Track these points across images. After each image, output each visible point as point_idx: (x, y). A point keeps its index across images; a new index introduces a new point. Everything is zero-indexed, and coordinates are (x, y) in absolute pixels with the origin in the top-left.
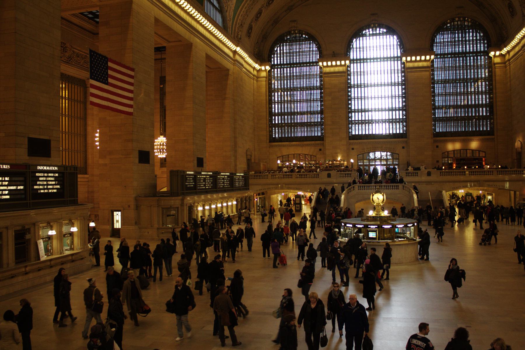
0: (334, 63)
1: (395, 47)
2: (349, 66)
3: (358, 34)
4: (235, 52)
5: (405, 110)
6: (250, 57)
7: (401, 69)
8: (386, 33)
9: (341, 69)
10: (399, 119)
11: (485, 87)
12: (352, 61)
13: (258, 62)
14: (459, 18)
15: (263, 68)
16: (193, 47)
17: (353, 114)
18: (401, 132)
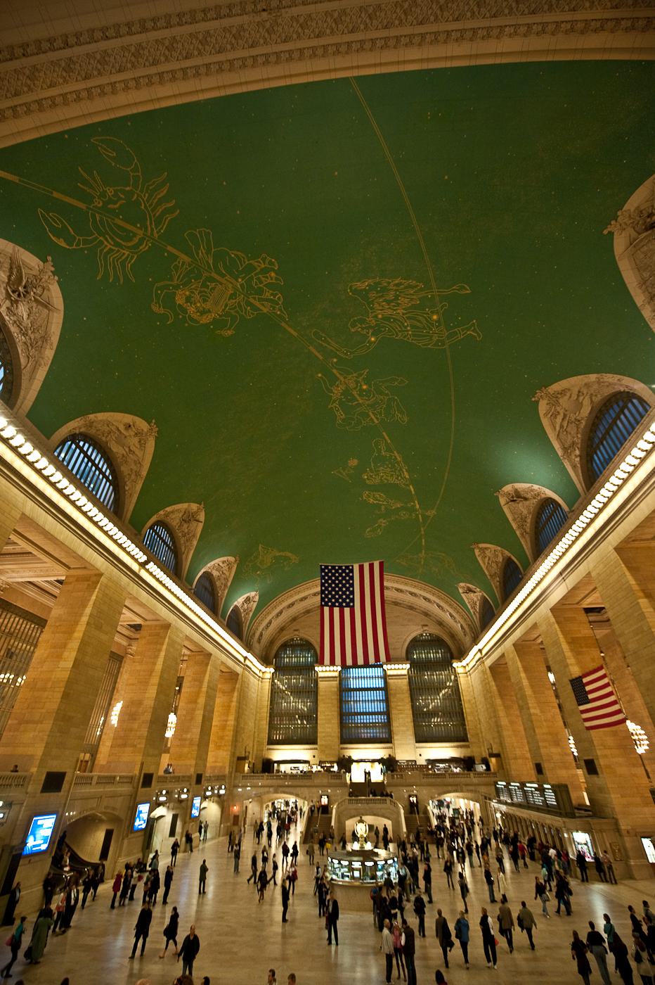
4: (246, 658)
14: (426, 634)
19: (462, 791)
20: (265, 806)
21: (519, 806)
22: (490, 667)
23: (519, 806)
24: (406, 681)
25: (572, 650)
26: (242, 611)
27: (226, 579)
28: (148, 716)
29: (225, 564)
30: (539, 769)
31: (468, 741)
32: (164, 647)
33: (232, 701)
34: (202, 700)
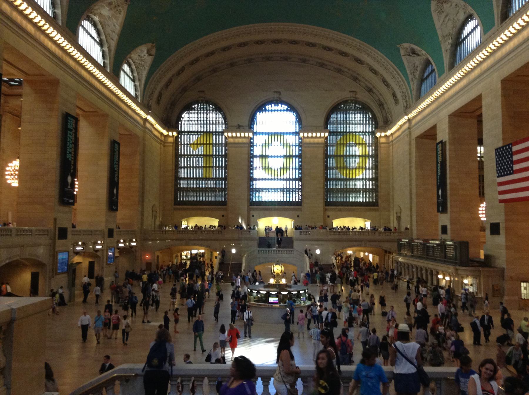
0: (238, 135)
1: (294, 123)
2: (253, 139)
3: (261, 108)
4: (146, 120)
5: (301, 181)
6: (159, 124)
7: (299, 144)
8: (287, 110)
9: (245, 141)
10: (296, 188)
11: (372, 163)
12: (255, 133)
13: (167, 128)
15: (170, 134)
17: (254, 182)
18: (297, 200)
20: (174, 255)
29: (112, 6)
31: (377, 206)
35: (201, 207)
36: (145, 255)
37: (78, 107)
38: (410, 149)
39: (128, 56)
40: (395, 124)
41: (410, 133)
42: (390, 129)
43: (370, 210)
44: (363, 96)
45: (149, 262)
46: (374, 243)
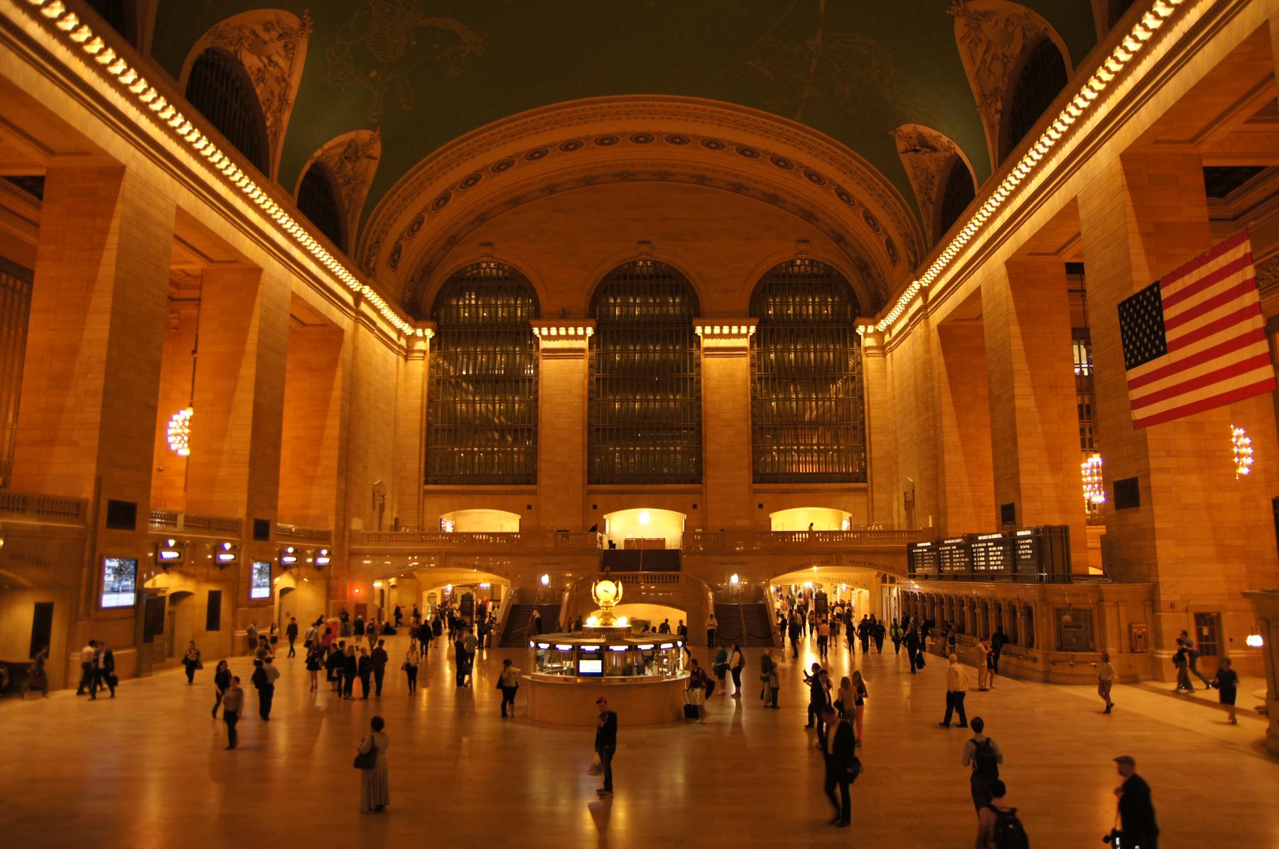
4: (358, 297)
6: (391, 307)
13: (410, 319)
15: (419, 332)
16: (264, 278)
19: (839, 563)
20: (425, 594)
21: (956, 577)
22: (940, 327)
23: (956, 577)
24: (743, 363)
25: (1148, 252)
26: (341, 181)
27: (283, 80)
28: (96, 381)
29: (274, 34)
30: (1008, 515)
32: (115, 223)
33: (331, 388)
34: (248, 371)
35: (483, 488)
36: (352, 588)
37: (176, 236)
38: (928, 351)
39: (318, 153)
40: (895, 304)
41: (926, 317)
42: (883, 318)
43: (850, 490)
44: (827, 254)
45: (362, 602)
46: (858, 558)
